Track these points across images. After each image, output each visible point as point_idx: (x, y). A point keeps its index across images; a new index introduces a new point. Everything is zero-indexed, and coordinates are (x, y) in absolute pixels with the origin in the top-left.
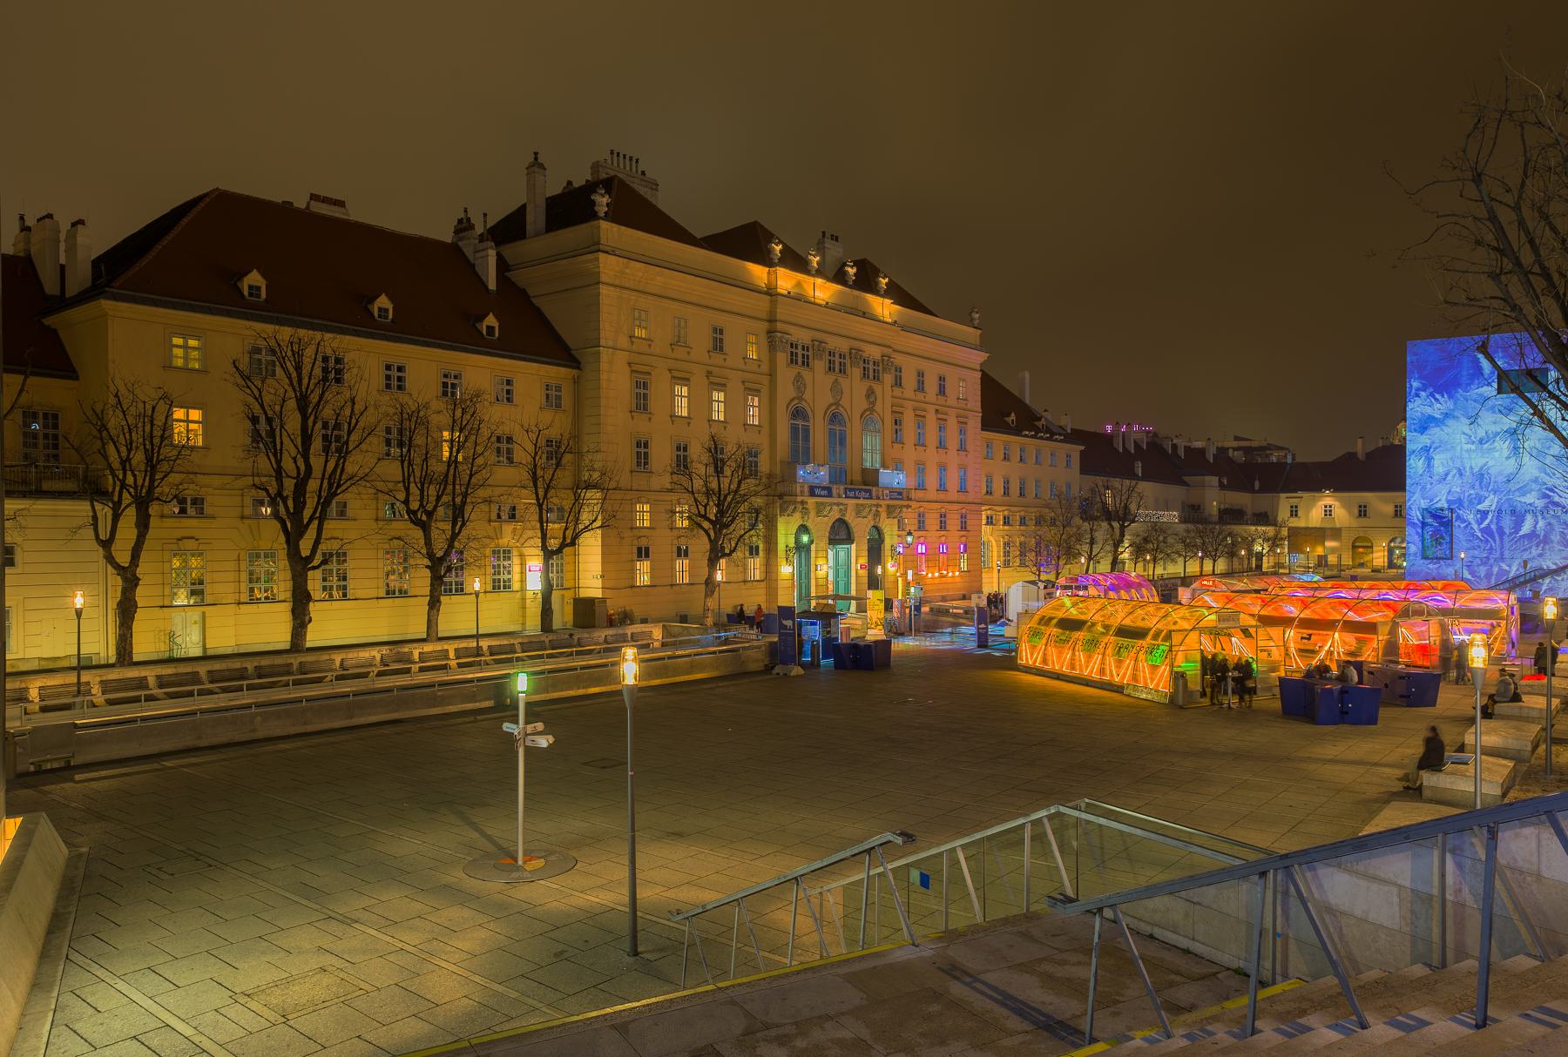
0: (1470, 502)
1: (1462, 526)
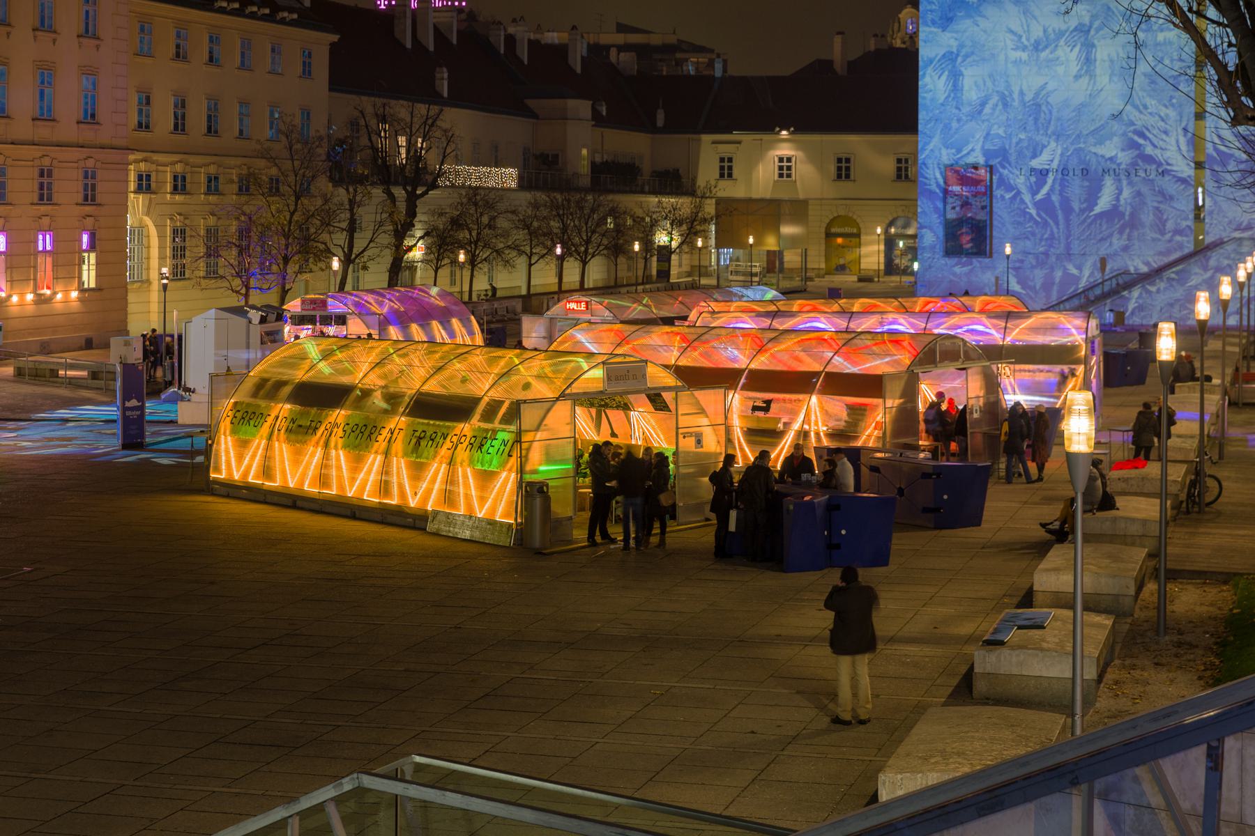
0: (1020, 154)
1: (1008, 196)
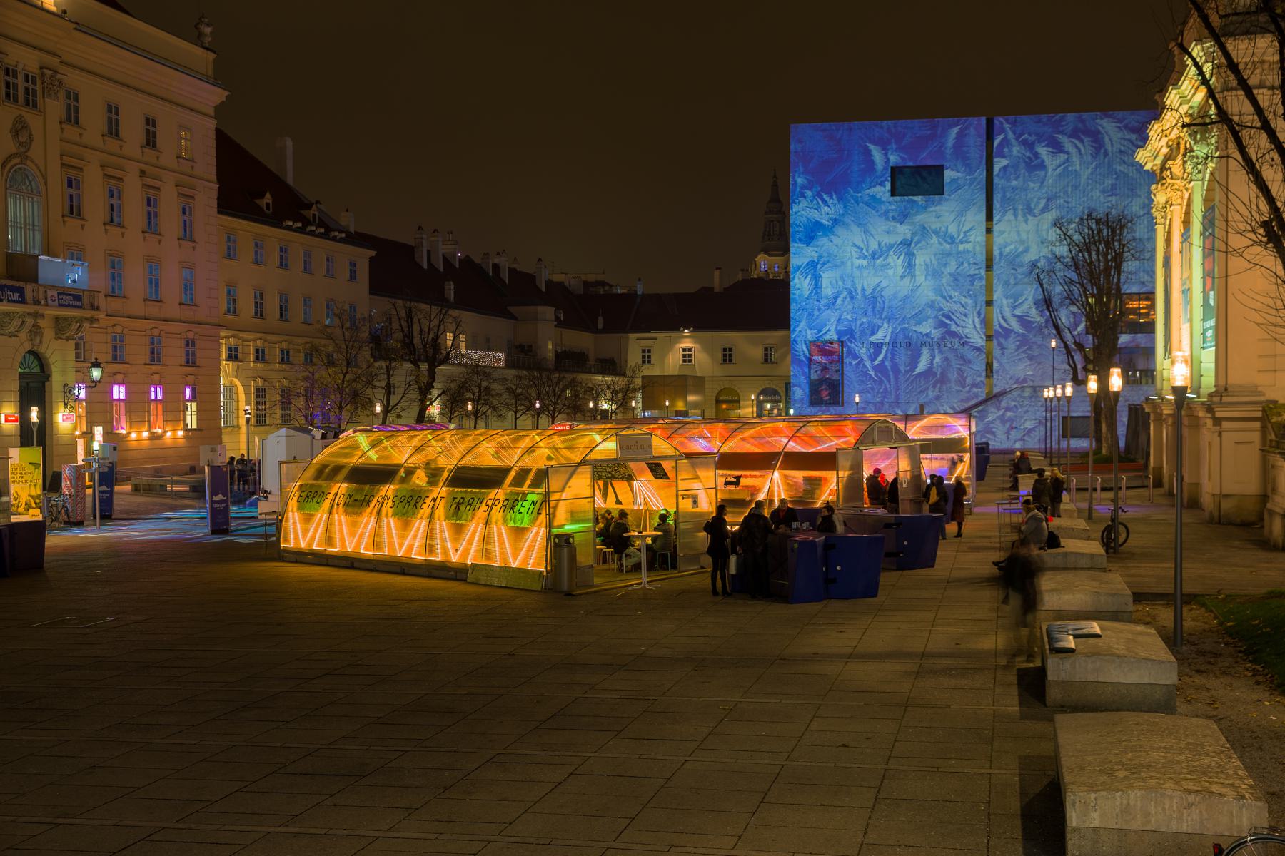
0: (862, 332)
